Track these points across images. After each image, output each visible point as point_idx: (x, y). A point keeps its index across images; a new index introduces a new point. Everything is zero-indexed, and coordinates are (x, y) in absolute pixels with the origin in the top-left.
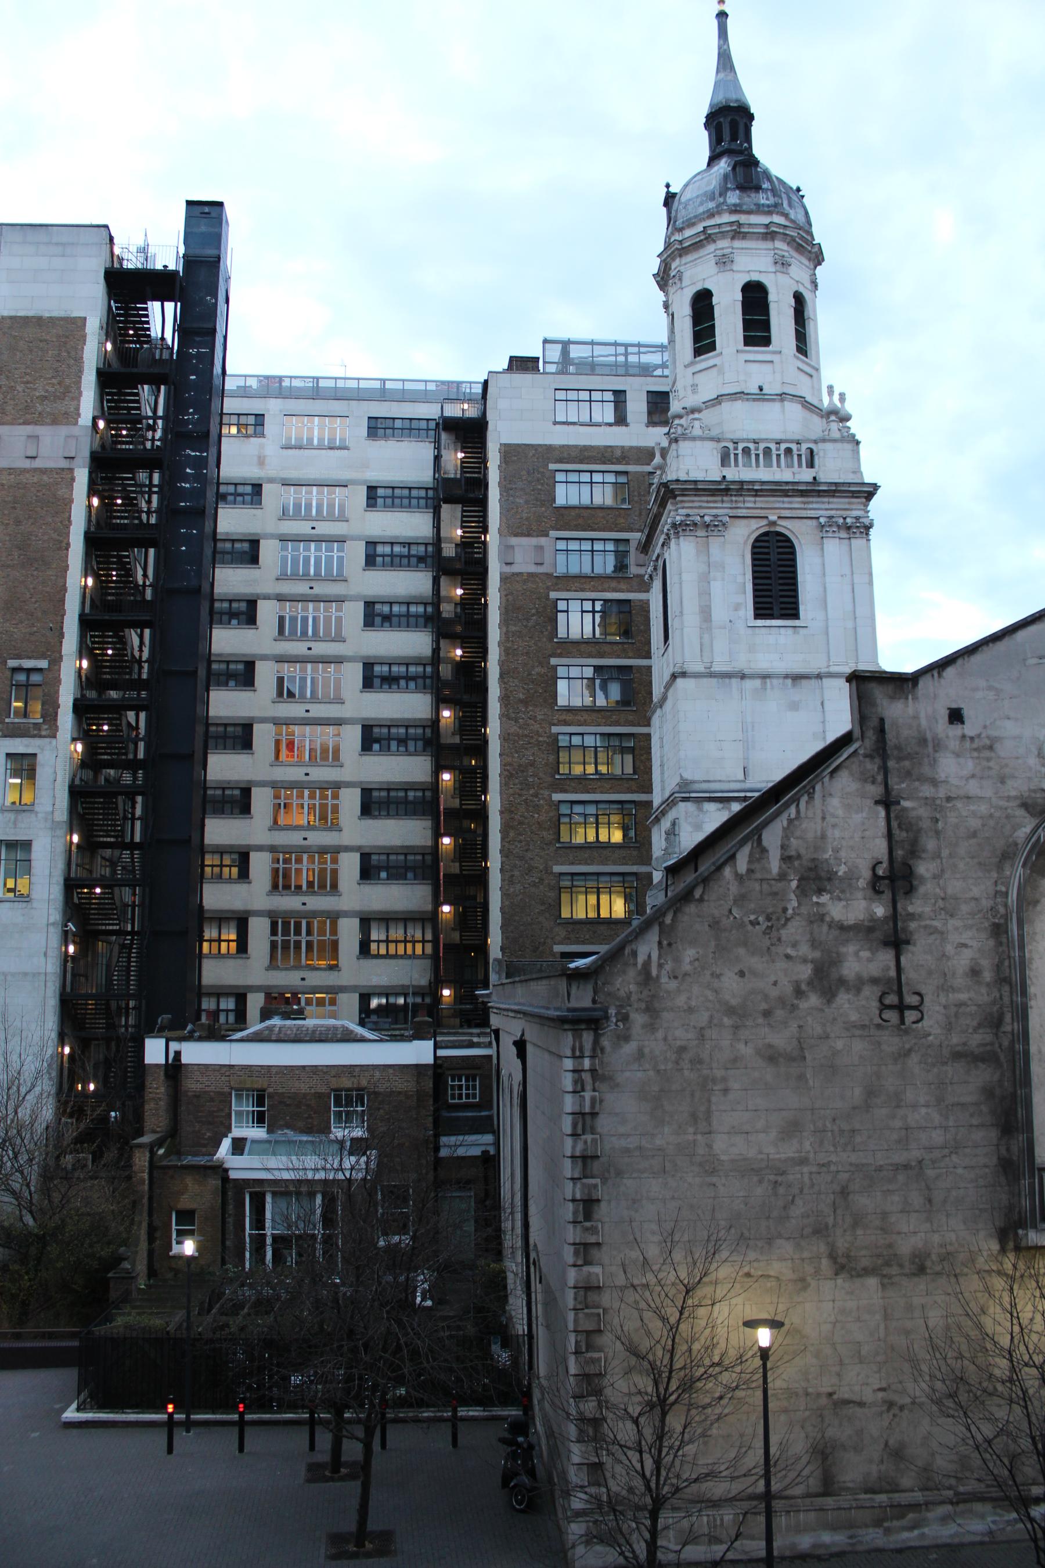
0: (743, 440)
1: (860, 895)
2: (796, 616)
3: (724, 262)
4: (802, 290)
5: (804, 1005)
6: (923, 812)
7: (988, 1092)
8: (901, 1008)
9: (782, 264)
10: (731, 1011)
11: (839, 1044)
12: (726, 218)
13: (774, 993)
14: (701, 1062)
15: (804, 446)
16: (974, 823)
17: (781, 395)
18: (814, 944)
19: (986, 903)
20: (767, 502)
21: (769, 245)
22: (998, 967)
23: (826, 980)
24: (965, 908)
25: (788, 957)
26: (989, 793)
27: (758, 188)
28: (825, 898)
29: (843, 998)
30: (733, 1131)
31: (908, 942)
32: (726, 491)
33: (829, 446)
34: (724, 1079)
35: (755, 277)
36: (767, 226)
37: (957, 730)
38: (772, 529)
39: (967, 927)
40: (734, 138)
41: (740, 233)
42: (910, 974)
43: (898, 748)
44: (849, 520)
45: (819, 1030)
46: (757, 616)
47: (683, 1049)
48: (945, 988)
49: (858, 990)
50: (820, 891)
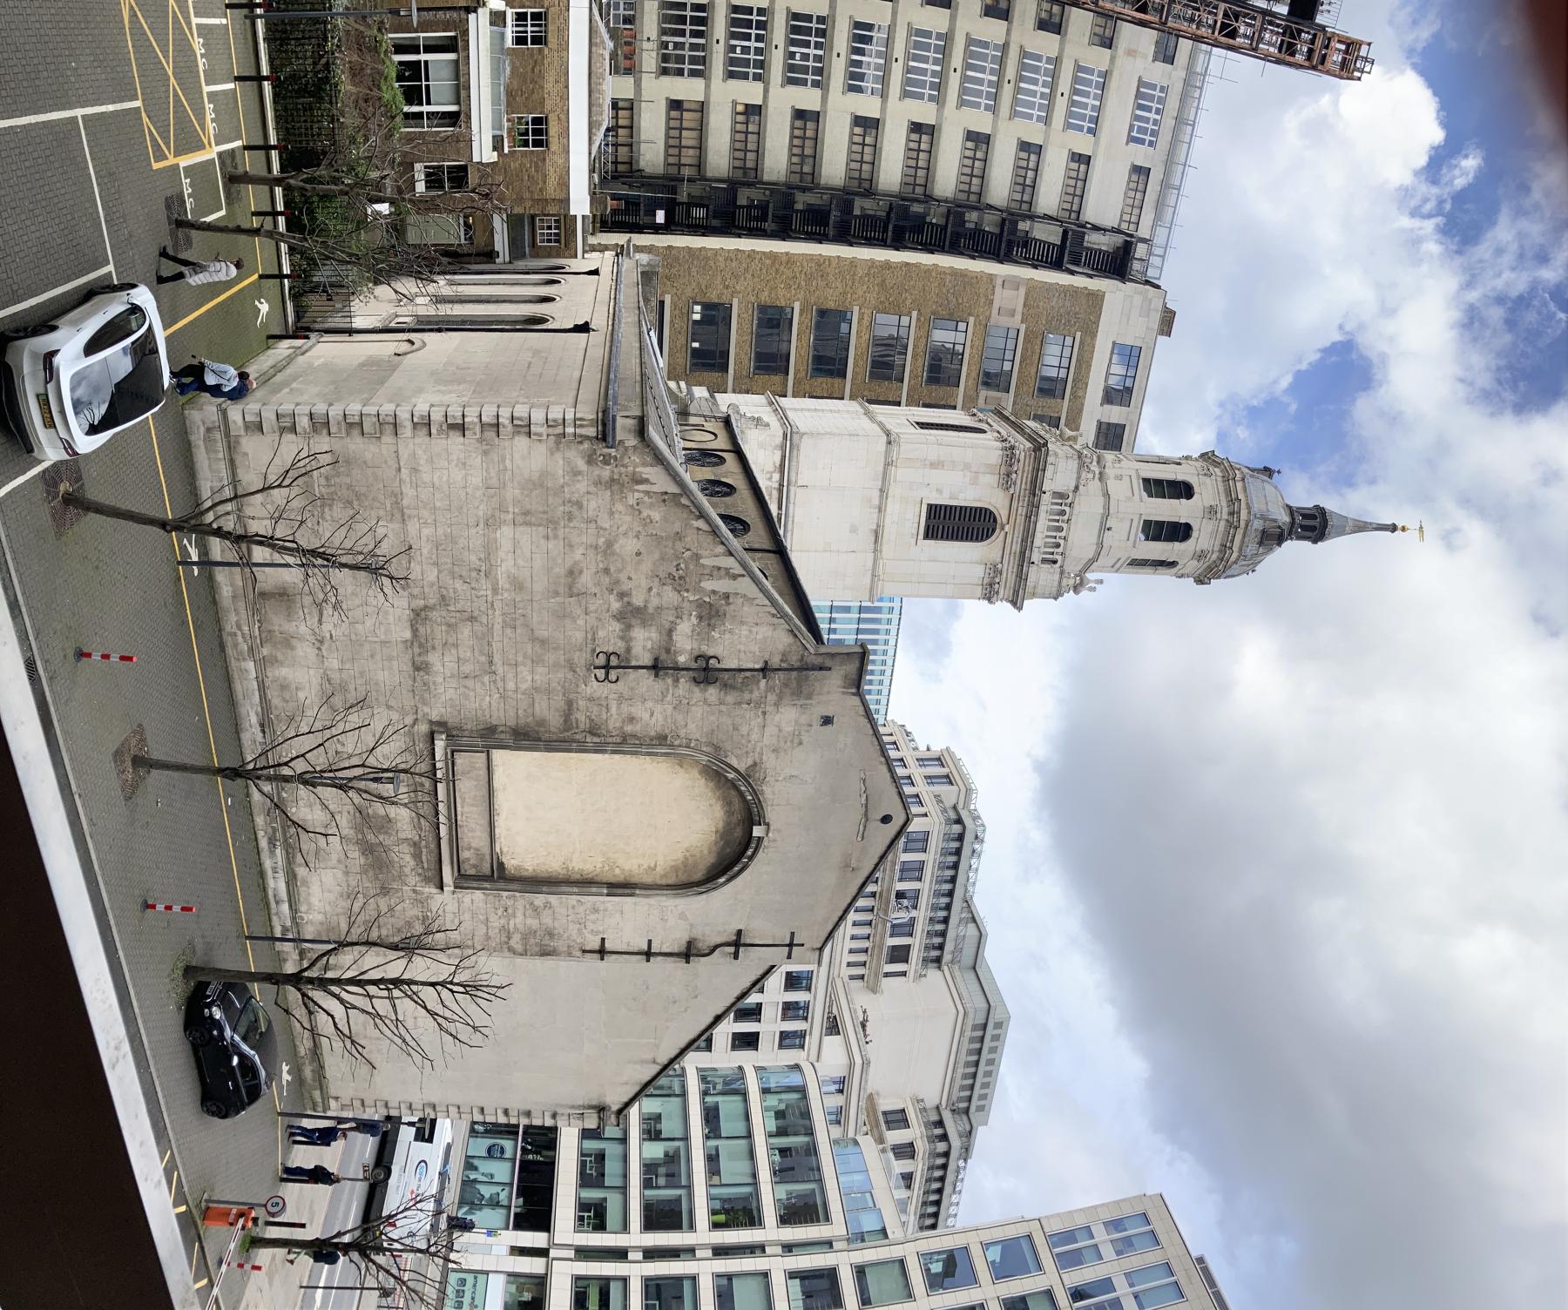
1: (695, 646)
2: (926, 537)
5: (612, 598)
6: (756, 695)
7: (542, 722)
8: (607, 667)
9: (1201, 556)
10: (609, 544)
11: (581, 622)
13: (623, 577)
14: (570, 520)
16: (744, 730)
18: (659, 608)
19: (682, 733)
22: (634, 736)
23: (631, 615)
24: (680, 718)
25: (650, 589)
26: (766, 741)
27: (1261, 543)
28: (694, 620)
29: (616, 626)
30: (515, 543)
31: (656, 676)
33: (1057, 577)
34: (556, 537)
35: (1195, 534)
37: (817, 722)
39: (665, 719)
40: (1303, 527)
42: (632, 674)
43: (807, 678)
45: (592, 608)
46: (930, 506)
47: (579, 505)
48: (621, 699)
49: (622, 638)
50: (700, 618)
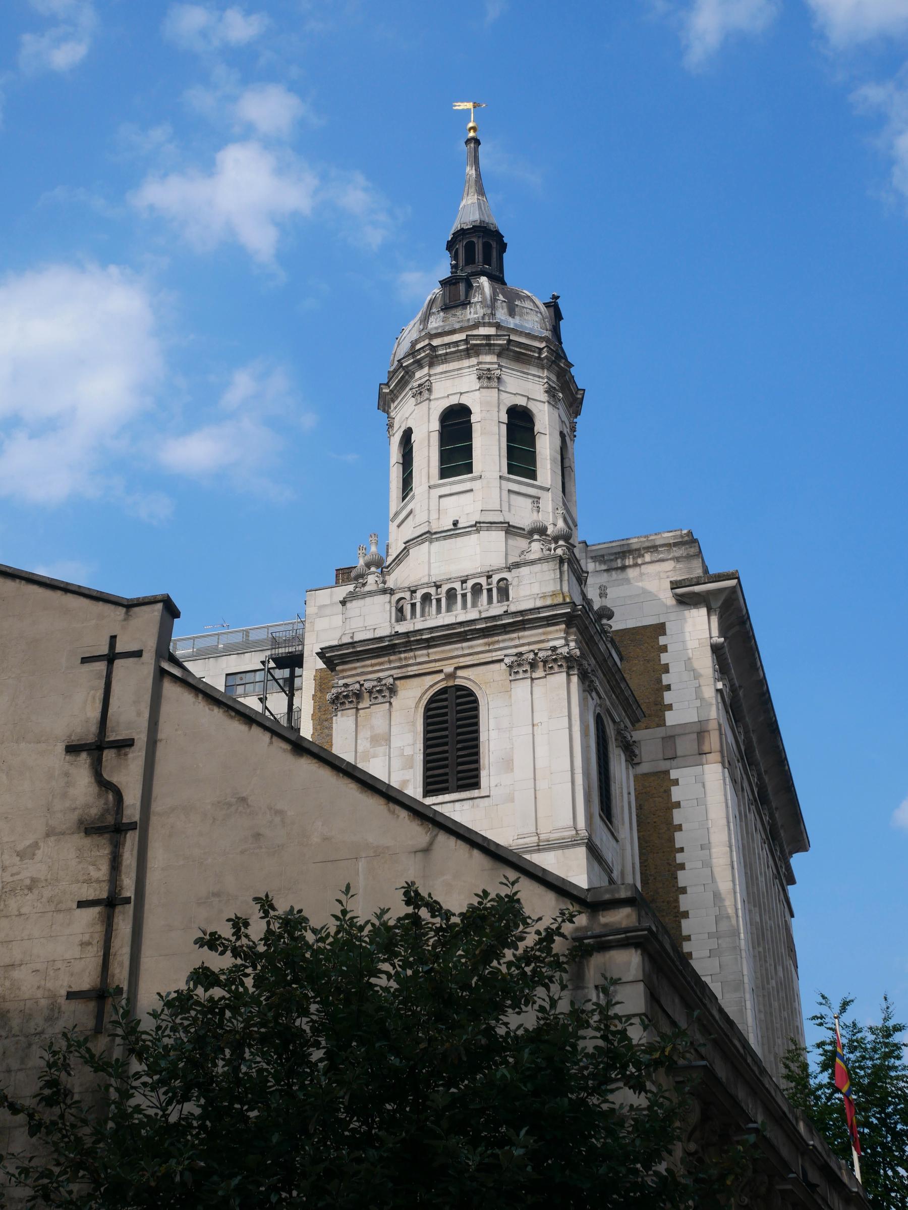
0: (423, 586)
15: (495, 578)
17: (475, 526)
20: (443, 652)
21: (474, 361)
27: (466, 304)
33: (524, 570)
35: (454, 400)
36: (466, 341)
38: (451, 684)
40: (487, 260)
41: (437, 356)
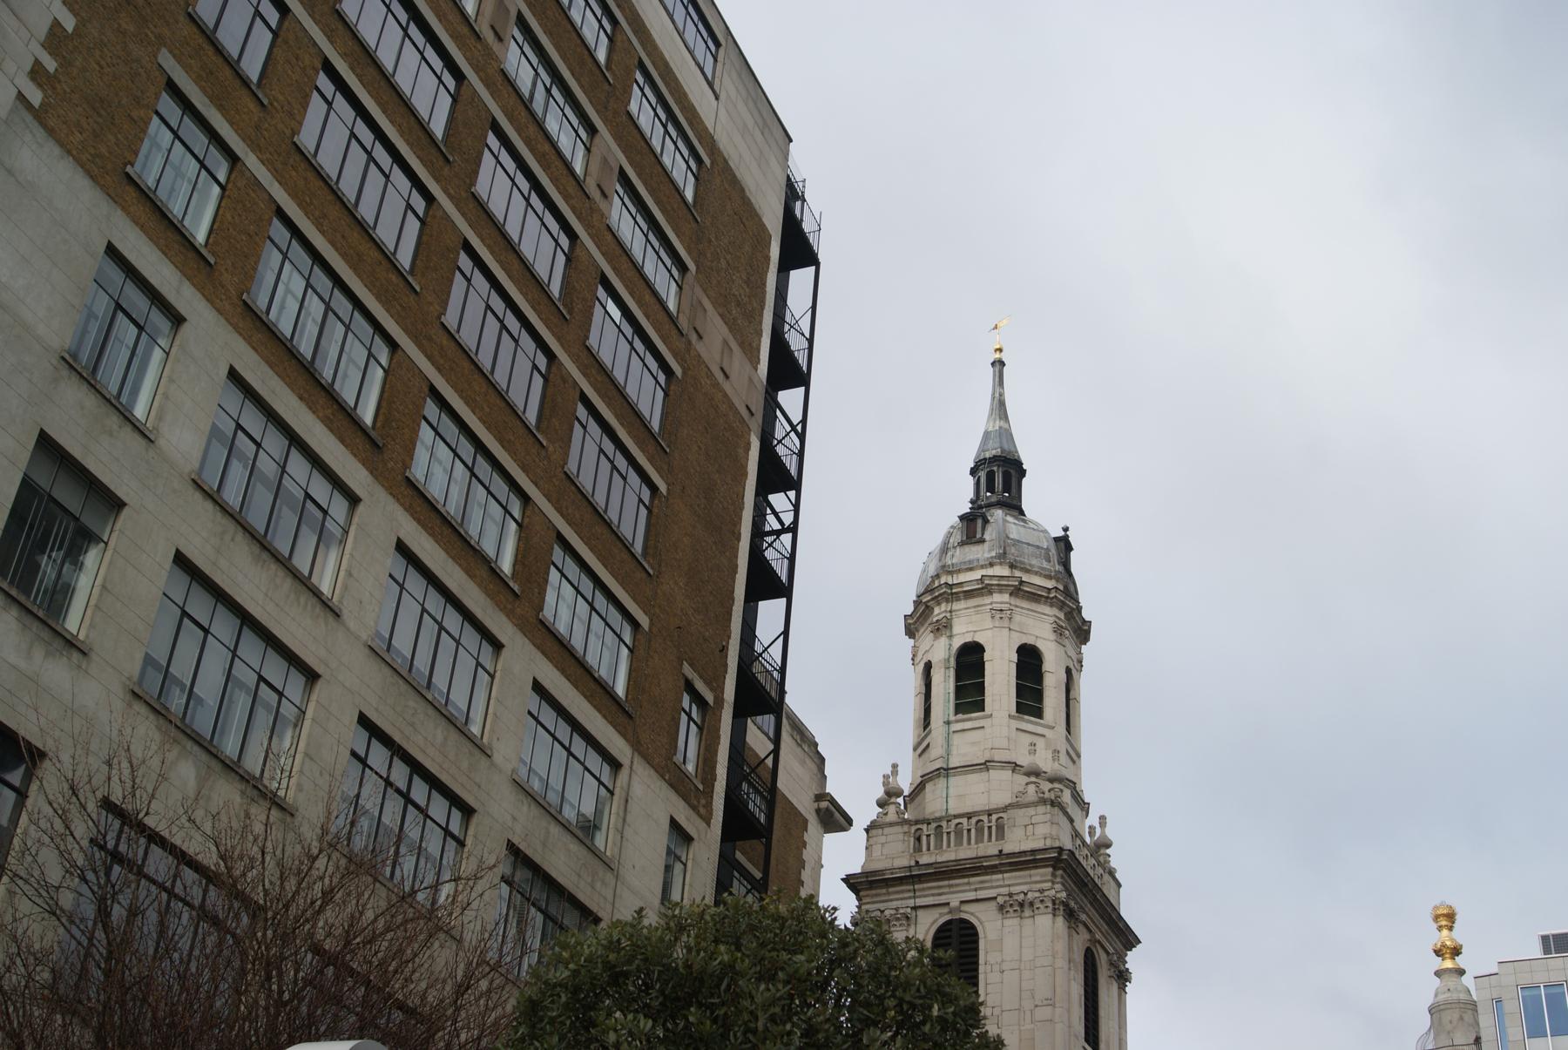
3: (943, 628)
4: (1030, 640)
12: (1005, 571)
32: (920, 878)
35: (968, 639)
36: (981, 580)
40: (1007, 487)
44: (1030, 895)
